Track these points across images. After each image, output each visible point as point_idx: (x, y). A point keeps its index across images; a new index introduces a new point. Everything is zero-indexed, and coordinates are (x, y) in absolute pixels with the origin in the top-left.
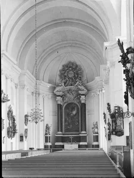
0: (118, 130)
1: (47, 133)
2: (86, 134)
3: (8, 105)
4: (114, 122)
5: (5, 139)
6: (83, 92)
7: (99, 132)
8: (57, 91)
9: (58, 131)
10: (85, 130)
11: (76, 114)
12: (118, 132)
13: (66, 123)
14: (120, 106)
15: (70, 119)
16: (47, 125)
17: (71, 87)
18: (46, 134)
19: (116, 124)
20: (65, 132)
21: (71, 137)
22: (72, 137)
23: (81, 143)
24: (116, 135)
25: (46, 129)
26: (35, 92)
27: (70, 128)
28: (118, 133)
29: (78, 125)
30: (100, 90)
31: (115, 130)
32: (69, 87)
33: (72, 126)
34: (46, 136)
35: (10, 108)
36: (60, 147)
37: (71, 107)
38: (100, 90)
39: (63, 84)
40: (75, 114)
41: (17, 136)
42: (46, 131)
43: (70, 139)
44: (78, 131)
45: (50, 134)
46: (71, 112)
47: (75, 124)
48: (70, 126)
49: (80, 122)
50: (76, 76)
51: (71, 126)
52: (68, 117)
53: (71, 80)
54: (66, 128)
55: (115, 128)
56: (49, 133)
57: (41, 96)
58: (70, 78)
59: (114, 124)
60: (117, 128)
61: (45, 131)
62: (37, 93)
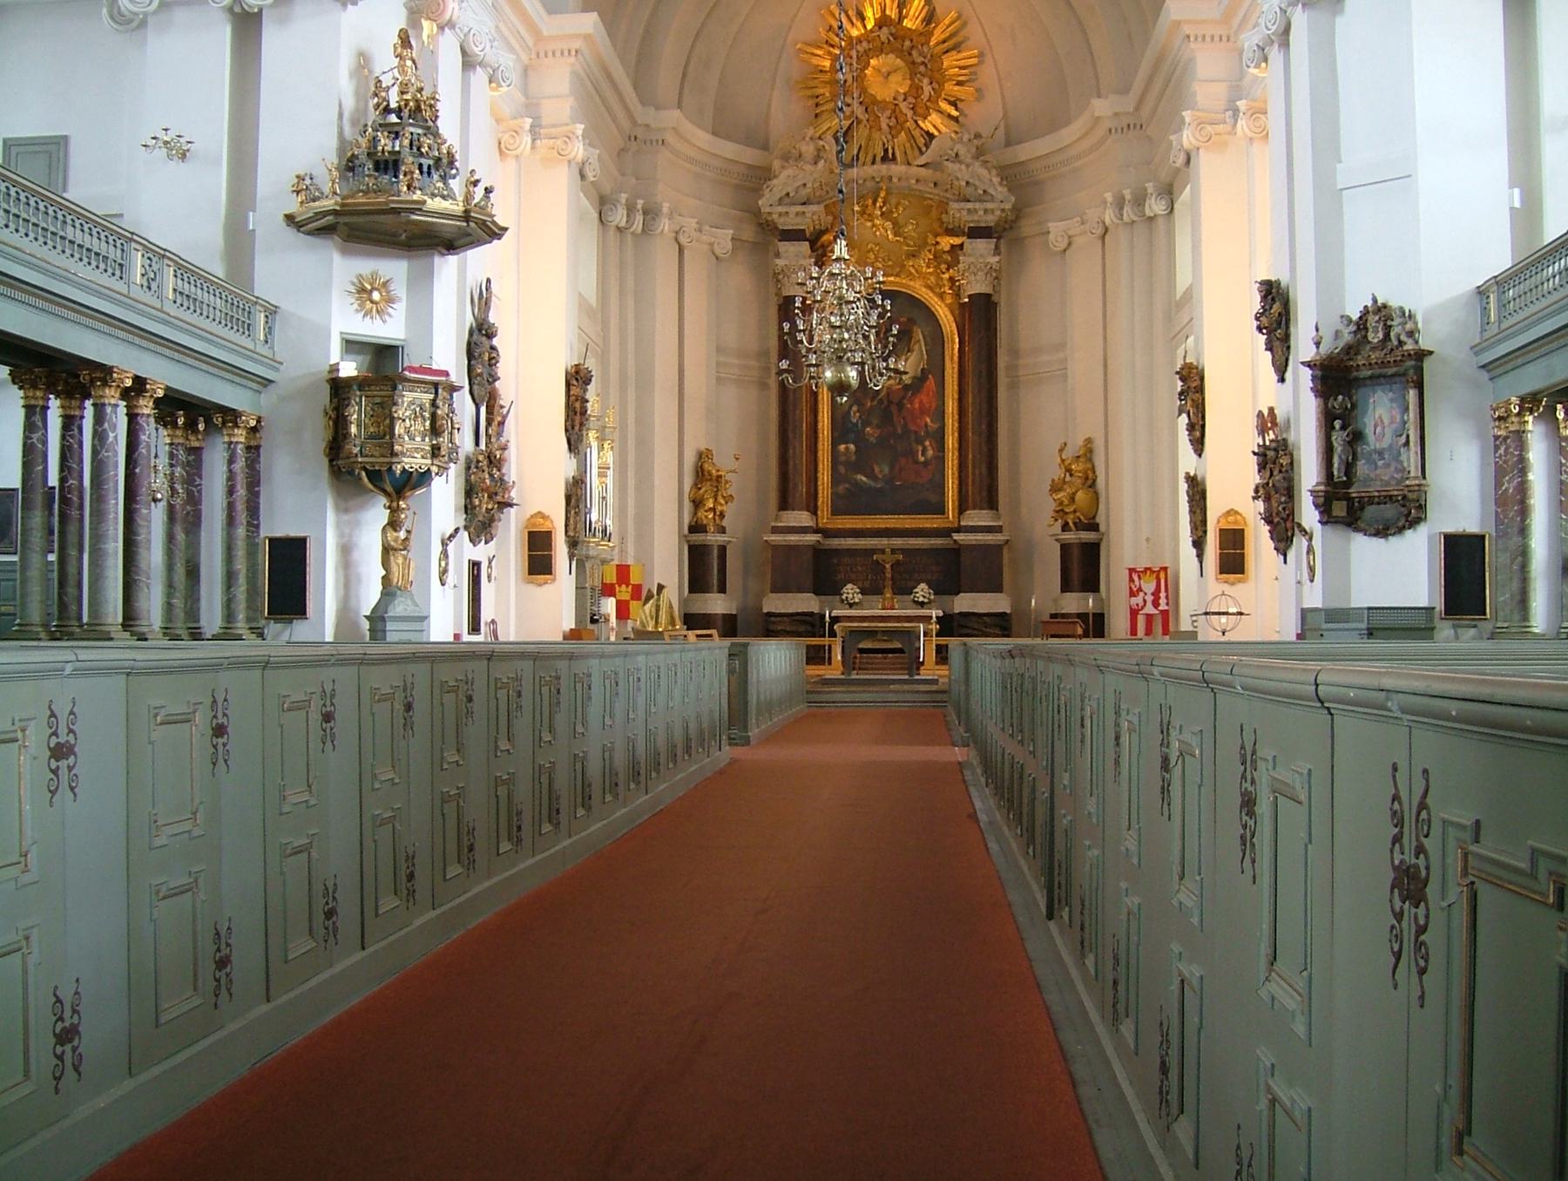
0: (1374, 489)
1: (706, 517)
2: (998, 529)
3: (475, 277)
4: (1337, 424)
5: (451, 547)
6: (986, 211)
7: (1100, 519)
8: (785, 199)
9: (784, 504)
10: (991, 503)
11: (920, 380)
12: (1371, 501)
13: (842, 447)
14: (1394, 303)
15: (875, 422)
16: (703, 456)
17: (882, 169)
18: (696, 528)
19: (1356, 437)
20: (836, 511)
21: (883, 551)
22: (893, 551)
23: (965, 603)
24: (1357, 530)
25: (696, 486)
26: (623, 197)
27: (873, 484)
28: (1370, 511)
29: (940, 459)
30: (1127, 194)
31: (1348, 484)
32: (870, 170)
33: (886, 470)
34: (698, 538)
35: (483, 300)
36: (802, 628)
38: (1127, 194)
39: (831, 147)
40: (914, 378)
41: (511, 527)
42: (697, 504)
43: (878, 567)
44: (940, 509)
45: (723, 530)
47: (913, 454)
48: (877, 469)
49: (951, 441)
50: (927, 89)
51: (882, 470)
53: (884, 126)
54: (841, 488)
55: (1349, 468)
56: (722, 515)
57: (665, 225)
58: (875, 102)
59: (1338, 439)
60: (1362, 468)
61: (687, 505)
62: (640, 203)
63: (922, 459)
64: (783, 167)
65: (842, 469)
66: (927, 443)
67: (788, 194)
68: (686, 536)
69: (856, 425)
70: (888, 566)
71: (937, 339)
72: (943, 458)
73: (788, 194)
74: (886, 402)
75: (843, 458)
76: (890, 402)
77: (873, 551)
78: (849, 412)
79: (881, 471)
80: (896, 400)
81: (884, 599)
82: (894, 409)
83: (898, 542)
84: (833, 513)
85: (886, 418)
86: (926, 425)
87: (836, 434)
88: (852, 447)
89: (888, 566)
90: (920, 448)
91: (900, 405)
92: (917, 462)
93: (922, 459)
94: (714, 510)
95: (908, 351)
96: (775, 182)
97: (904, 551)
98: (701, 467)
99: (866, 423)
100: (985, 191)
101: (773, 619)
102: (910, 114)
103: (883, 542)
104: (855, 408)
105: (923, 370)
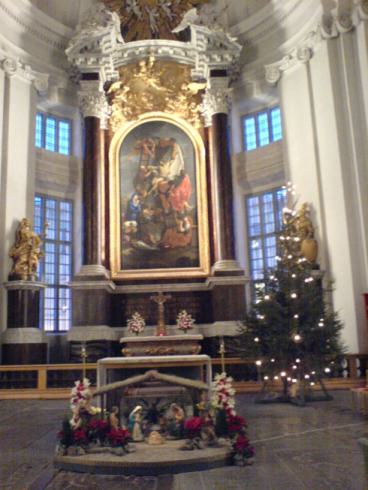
11: (180, 177)
13: (127, 223)
15: (150, 204)
21: (157, 294)
22: (165, 293)
33: (158, 237)
37: (154, 144)
40: (176, 176)
43: (154, 306)
44: (196, 263)
46: (154, 169)
47: (176, 226)
48: (152, 237)
52: (140, 194)
53: (152, 19)
54: (127, 251)
63: (183, 230)
64: (83, 28)
65: (128, 238)
66: (186, 219)
67: (86, 48)
68: (5, 284)
69: (137, 208)
70: (161, 303)
71: (191, 152)
72: (197, 229)
73: (86, 48)
74: (157, 194)
75: (128, 231)
76: (160, 192)
77: (147, 295)
78: (131, 200)
79: (155, 239)
80: (163, 191)
81: (158, 329)
82: (163, 197)
83: (168, 287)
84: (122, 268)
85: (158, 203)
86: (185, 207)
87: (123, 215)
88: (135, 223)
89: (161, 303)
90: (181, 223)
91: (167, 195)
92: (179, 232)
93: (183, 230)
94: (27, 263)
95: (172, 159)
96: (76, 38)
97: (173, 294)
98: (20, 232)
99: (144, 207)
100: (221, 45)
101: (75, 346)
102: (168, 11)
103: (158, 288)
104: (136, 197)
105: (182, 171)
